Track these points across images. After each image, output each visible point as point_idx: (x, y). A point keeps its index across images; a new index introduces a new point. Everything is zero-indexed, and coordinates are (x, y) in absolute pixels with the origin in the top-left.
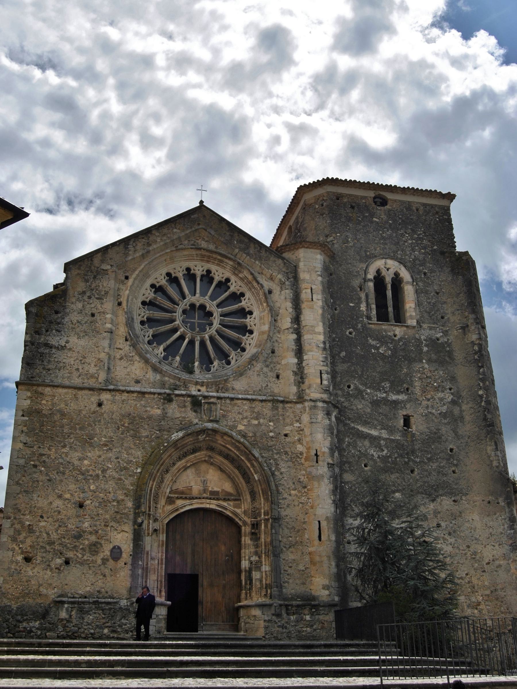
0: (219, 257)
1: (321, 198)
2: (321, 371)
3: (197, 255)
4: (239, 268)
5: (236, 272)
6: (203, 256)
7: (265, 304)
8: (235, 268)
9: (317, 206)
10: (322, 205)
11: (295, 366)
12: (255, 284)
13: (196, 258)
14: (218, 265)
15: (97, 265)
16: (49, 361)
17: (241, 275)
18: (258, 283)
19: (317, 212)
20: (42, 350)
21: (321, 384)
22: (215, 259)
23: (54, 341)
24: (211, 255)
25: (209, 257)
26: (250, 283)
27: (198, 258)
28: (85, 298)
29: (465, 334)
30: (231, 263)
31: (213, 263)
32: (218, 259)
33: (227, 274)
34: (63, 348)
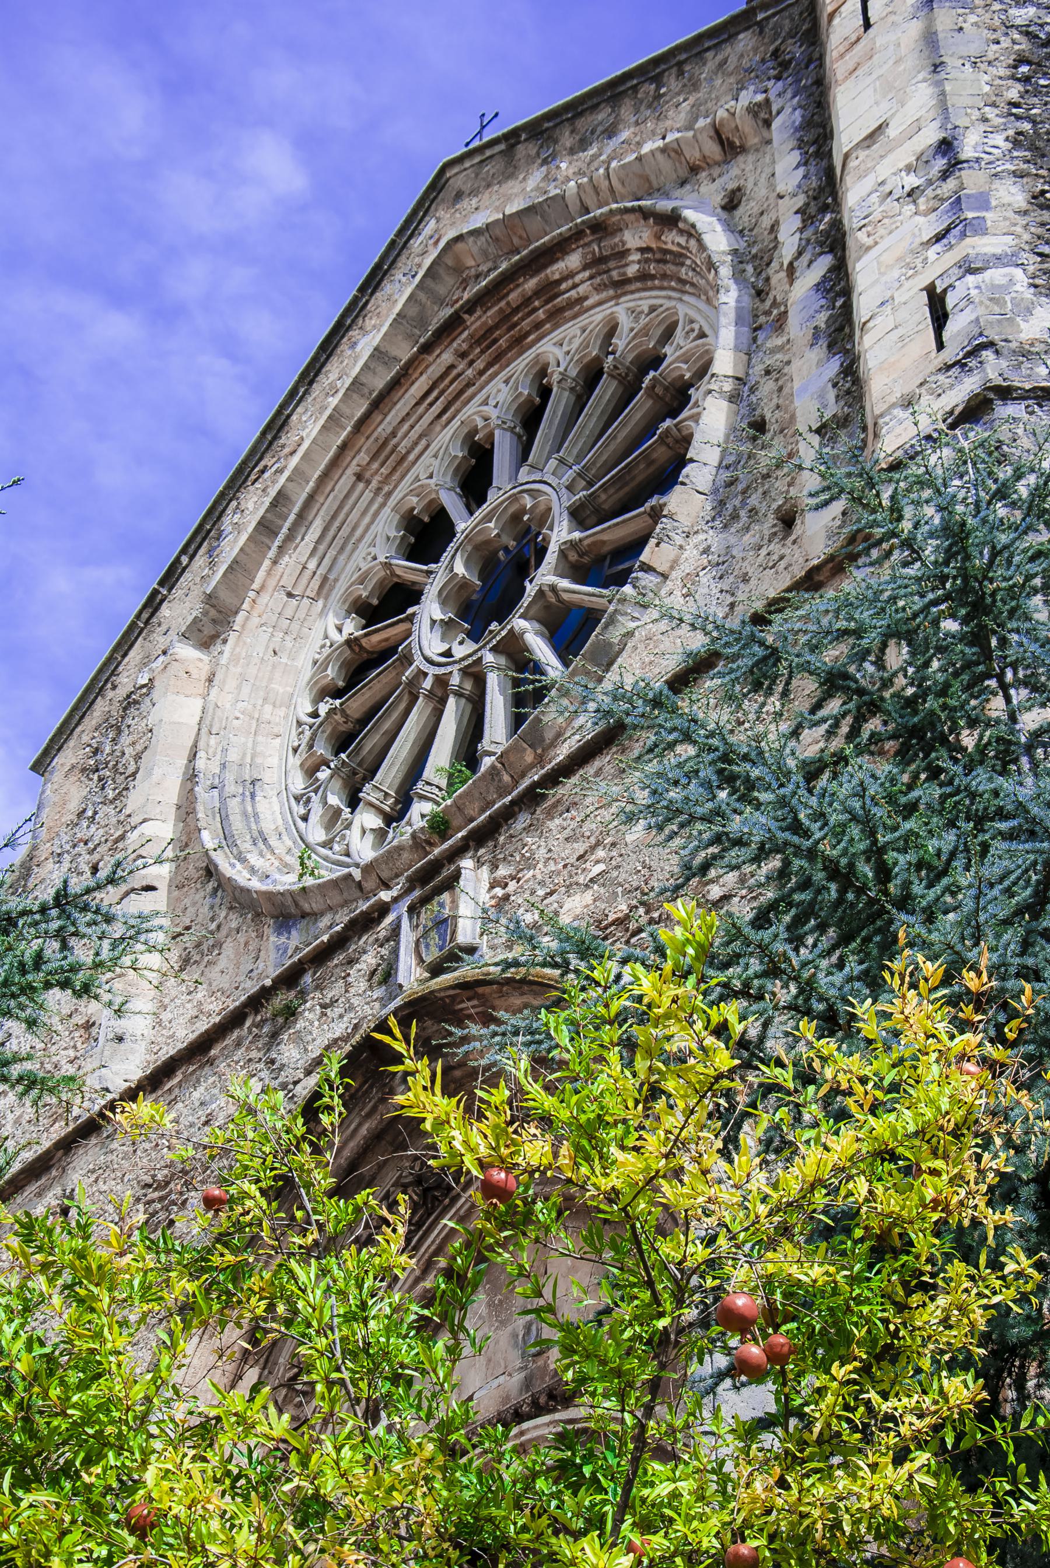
0: (531, 284)
2: (930, 290)
3: (463, 355)
5: (615, 274)
6: (484, 338)
11: (831, 394)
13: (469, 372)
14: (557, 316)
21: (940, 346)
22: (527, 301)
24: (503, 304)
25: (505, 319)
27: (480, 364)
30: (573, 260)
31: (538, 326)
32: (537, 293)
33: (599, 317)
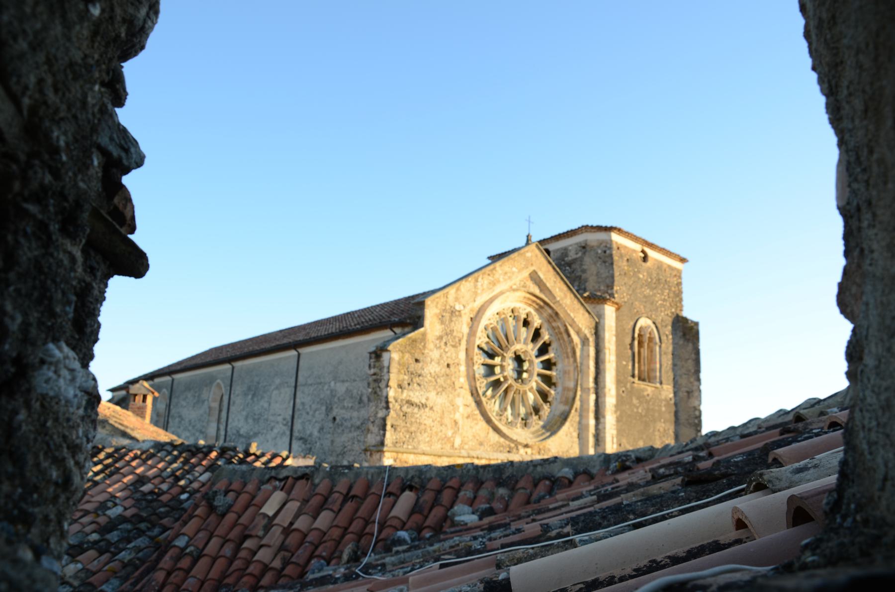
1: (604, 244)
4: (556, 318)
7: (571, 360)
8: (551, 316)
9: (599, 251)
10: (605, 252)
12: (565, 336)
15: (452, 304)
16: (411, 423)
17: (554, 324)
18: (569, 335)
19: (600, 258)
20: (405, 408)
23: (416, 395)
26: (561, 333)
28: (442, 344)
29: (689, 397)
30: (550, 311)
34: (424, 406)
